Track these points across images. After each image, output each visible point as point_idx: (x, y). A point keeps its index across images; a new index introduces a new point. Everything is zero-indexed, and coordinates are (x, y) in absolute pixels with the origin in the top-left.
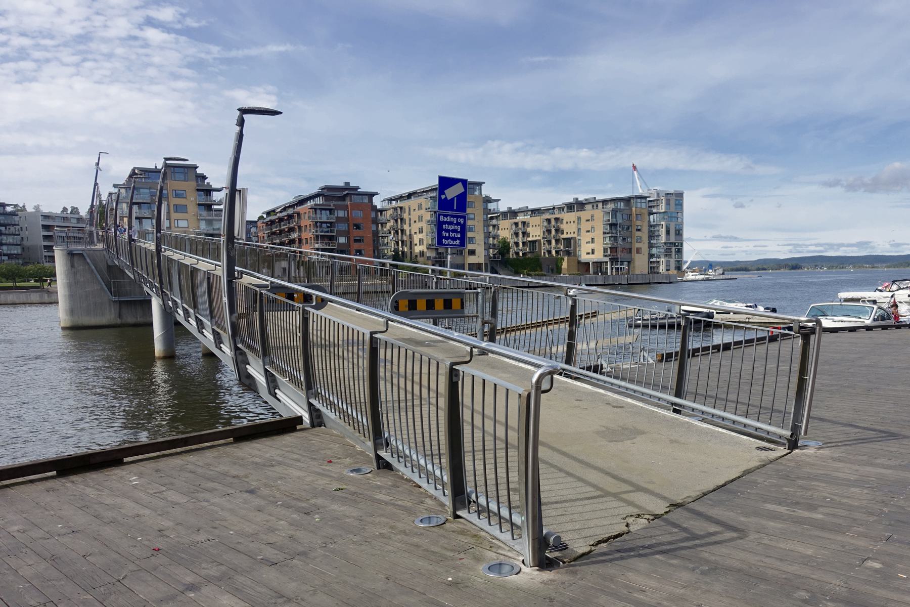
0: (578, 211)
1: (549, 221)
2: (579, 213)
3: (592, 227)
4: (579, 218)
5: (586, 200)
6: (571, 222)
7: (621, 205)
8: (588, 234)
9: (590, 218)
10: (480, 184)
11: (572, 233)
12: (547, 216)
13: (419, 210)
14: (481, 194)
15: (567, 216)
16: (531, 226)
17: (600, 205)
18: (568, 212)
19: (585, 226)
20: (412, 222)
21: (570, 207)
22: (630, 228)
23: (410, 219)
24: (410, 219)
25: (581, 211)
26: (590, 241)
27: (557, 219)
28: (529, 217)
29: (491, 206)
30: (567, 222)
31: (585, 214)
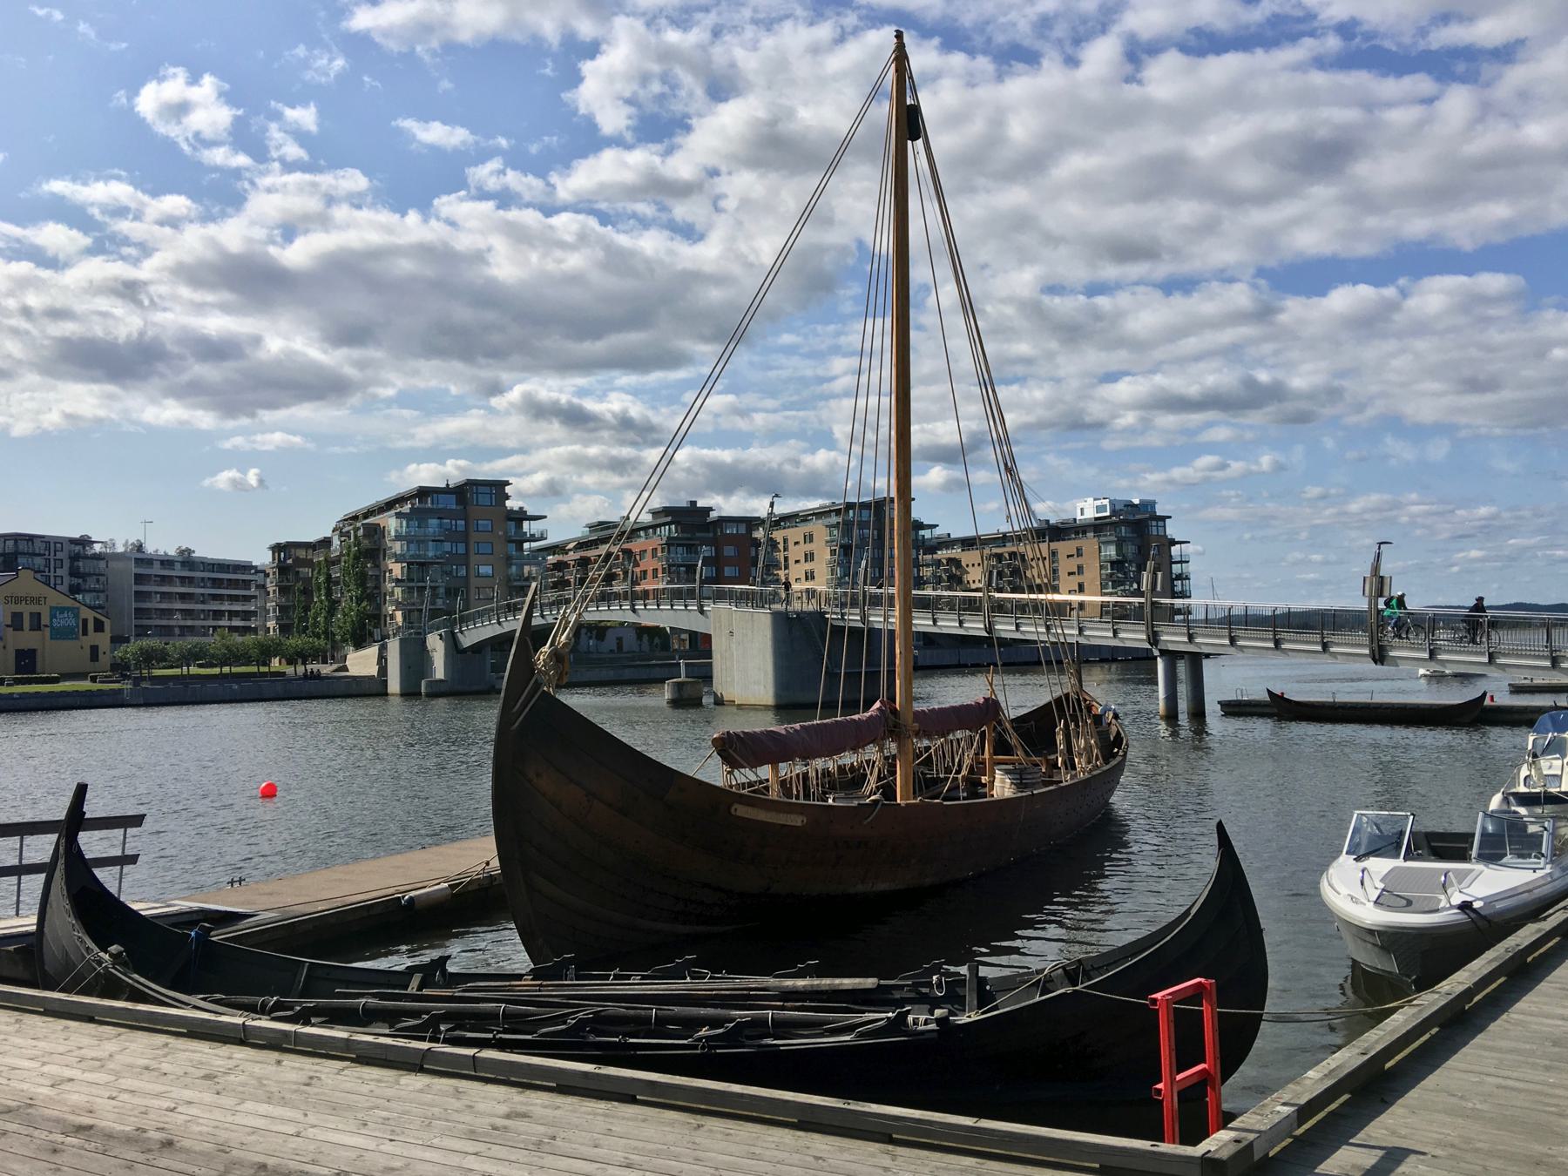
1: (999, 557)
2: (1054, 545)
3: (1080, 568)
4: (1054, 554)
5: (1062, 523)
8: (1072, 577)
9: (1075, 552)
19: (1065, 566)
20: (791, 562)
24: (786, 559)
26: (1077, 588)
28: (959, 550)
29: (926, 534)
31: (1064, 547)
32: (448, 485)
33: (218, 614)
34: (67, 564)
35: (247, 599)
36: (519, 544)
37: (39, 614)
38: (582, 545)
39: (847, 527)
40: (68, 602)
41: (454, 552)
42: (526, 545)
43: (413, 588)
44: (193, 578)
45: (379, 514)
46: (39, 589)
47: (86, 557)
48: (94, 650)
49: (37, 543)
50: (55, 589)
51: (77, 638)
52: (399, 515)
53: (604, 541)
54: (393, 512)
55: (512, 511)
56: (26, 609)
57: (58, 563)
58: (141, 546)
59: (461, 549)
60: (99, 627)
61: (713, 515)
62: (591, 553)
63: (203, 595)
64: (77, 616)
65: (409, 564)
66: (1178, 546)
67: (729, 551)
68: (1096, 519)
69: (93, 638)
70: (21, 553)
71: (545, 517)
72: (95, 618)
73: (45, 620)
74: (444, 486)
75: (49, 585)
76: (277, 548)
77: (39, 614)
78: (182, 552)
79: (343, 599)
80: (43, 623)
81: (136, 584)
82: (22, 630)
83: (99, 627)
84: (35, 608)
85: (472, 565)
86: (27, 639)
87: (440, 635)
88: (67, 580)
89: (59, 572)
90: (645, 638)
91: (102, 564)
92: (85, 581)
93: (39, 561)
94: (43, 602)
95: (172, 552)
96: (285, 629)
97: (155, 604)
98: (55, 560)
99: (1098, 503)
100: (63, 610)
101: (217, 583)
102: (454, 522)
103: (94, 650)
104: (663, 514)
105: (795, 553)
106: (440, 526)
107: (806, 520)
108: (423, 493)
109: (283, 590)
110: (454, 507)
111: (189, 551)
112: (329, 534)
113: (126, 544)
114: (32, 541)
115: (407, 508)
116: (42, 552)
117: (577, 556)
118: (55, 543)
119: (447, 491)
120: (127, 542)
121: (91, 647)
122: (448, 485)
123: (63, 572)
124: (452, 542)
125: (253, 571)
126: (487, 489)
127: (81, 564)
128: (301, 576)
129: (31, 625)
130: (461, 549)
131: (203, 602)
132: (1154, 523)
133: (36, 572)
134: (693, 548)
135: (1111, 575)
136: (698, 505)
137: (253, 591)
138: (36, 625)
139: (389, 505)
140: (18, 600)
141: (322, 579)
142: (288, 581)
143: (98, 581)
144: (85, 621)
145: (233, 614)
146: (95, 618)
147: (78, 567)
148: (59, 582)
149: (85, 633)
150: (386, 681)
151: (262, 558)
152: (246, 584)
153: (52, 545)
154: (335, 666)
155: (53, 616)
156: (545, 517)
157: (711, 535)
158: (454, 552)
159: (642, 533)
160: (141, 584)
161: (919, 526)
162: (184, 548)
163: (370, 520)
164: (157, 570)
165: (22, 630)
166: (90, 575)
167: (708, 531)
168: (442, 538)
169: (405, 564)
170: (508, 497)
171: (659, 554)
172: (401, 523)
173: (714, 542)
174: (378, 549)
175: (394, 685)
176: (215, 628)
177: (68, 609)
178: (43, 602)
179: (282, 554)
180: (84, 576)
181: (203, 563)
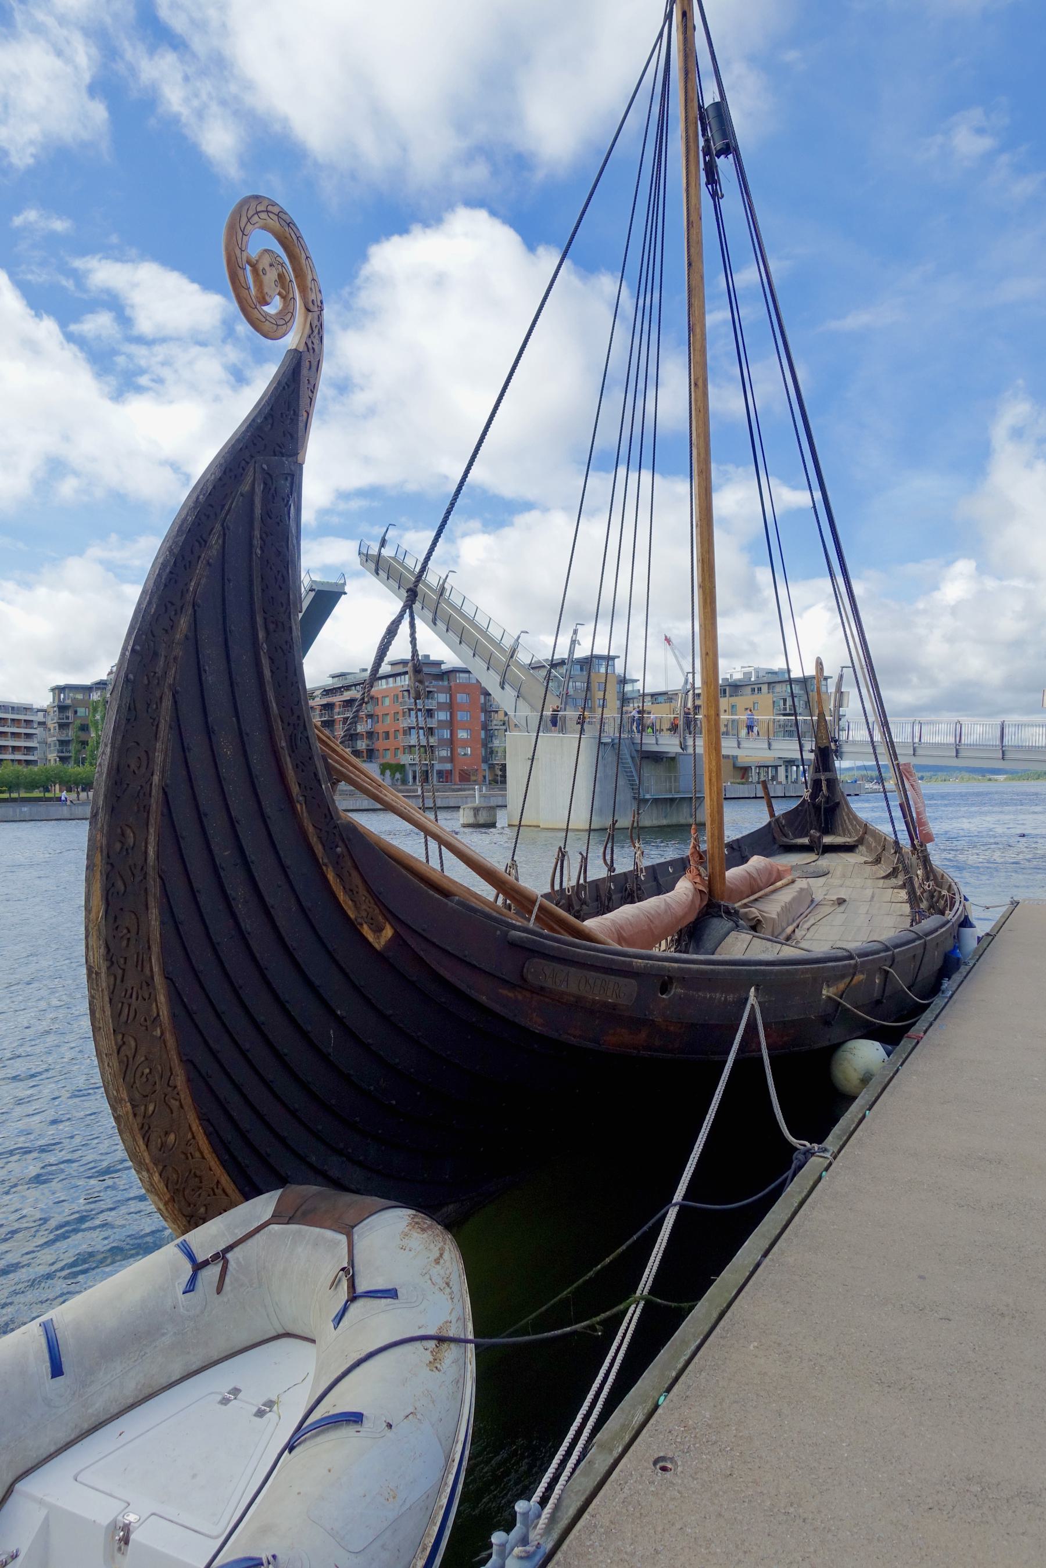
0: (731, 696)
35: (28, 736)
38: (328, 692)
53: (348, 688)
61: (443, 667)
62: (336, 699)
67: (461, 698)
76: (59, 690)
90: (388, 772)
96: (63, 760)
104: (401, 665)
109: (62, 726)
112: (105, 677)
117: (325, 701)
128: (79, 714)
134: (430, 695)
136: (431, 658)
142: (67, 718)
145: (15, 749)
151: (44, 700)
157: (446, 683)
159: (384, 681)
161: (623, 681)
167: (442, 680)
171: (400, 700)
173: (449, 690)
179: (62, 696)
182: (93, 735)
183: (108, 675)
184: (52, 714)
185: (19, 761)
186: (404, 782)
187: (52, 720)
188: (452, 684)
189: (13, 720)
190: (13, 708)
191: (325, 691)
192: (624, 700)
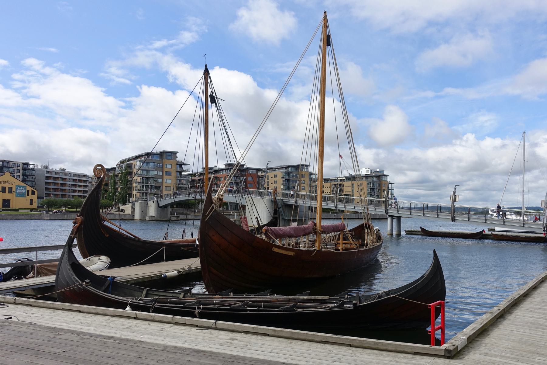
2: (353, 182)
6: (348, 186)
7: (375, 179)
10: (307, 166)
11: (349, 192)
12: (333, 183)
13: (275, 177)
14: (308, 171)
15: (346, 183)
16: (324, 187)
17: (364, 179)
18: (346, 181)
19: (356, 189)
20: (270, 183)
21: (348, 179)
22: (380, 191)
23: (268, 182)
25: (354, 181)
27: (340, 185)
30: (346, 186)
32: (157, 152)
33: (74, 191)
34: (21, 171)
36: (180, 173)
37: (12, 188)
39: (288, 173)
40: (23, 184)
41: (158, 174)
42: (183, 173)
43: (144, 185)
44: (66, 178)
45: (133, 160)
46: (12, 179)
47: (29, 170)
48: (31, 201)
49: (11, 163)
50: (17, 179)
51: (25, 197)
52: (140, 161)
54: (138, 160)
55: (178, 162)
56: (7, 186)
57: (18, 171)
58: (47, 167)
59: (161, 173)
60: (33, 193)
63: (70, 184)
64: (25, 189)
65: (143, 177)
66: (391, 184)
68: (366, 175)
69: (31, 197)
70: (5, 167)
71: (190, 164)
72: (32, 190)
73: (14, 190)
74: (156, 152)
75: (15, 177)
77: (12, 188)
78: (62, 170)
79: (119, 188)
80: (13, 191)
81: (46, 179)
82: (5, 193)
83: (33, 193)
84: (10, 186)
85: (164, 179)
86: (7, 196)
87: (153, 201)
88: (21, 177)
89: (18, 174)
91: (34, 172)
92: (28, 177)
93: (11, 170)
94: (13, 184)
95: (58, 169)
97: (52, 186)
98: (17, 170)
99: (367, 170)
100: (20, 187)
101: (74, 180)
102: (158, 164)
103: (31, 201)
105: (271, 180)
106: (154, 165)
107: (275, 170)
108: (148, 154)
110: (158, 159)
111: (64, 170)
112: (115, 166)
113: (42, 166)
114: (9, 163)
115: (143, 159)
116: (12, 167)
117: (199, 178)
118: (17, 164)
119: (156, 154)
120: (42, 165)
121: (30, 200)
122: (157, 152)
123: (20, 174)
124: (158, 171)
125: (88, 177)
126: (170, 154)
127: (26, 171)
129: (9, 191)
130: (161, 173)
131: (69, 187)
132: (384, 177)
133: (11, 173)
135: (370, 193)
137: (87, 184)
138: (11, 190)
139: (137, 157)
140: (4, 182)
141: (112, 181)
143: (32, 177)
144: (28, 191)
145: (79, 191)
146: (32, 190)
147: (25, 172)
148: (18, 177)
149: (28, 195)
150: (134, 216)
152: (85, 181)
153: (16, 164)
154: (116, 210)
155: (17, 189)
156: (190, 164)
158: (158, 174)
160: (48, 179)
161: (311, 174)
162: (62, 168)
163: (130, 162)
164: (54, 175)
165: (5, 193)
166: (30, 175)
167: (243, 172)
168: (154, 169)
169: (142, 178)
170: (177, 157)
172: (141, 164)
174: (132, 172)
175: (137, 216)
176: (73, 196)
177: (22, 186)
178: (13, 184)
180: (27, 176)
181: (70, 174)
182: (110, 188)
183: (117, 165)
184: (94, 179)
185: (81, 196)
186: (227, 209)
187: (94, 181)
188: (246, 173)
189: (79, 180)
190: (79, 175)
191: (200, 174)
192: (311, 180)
